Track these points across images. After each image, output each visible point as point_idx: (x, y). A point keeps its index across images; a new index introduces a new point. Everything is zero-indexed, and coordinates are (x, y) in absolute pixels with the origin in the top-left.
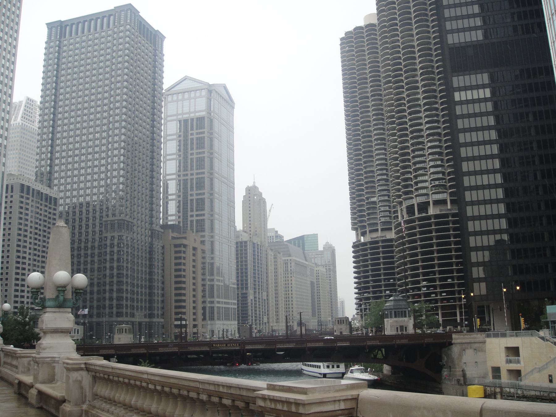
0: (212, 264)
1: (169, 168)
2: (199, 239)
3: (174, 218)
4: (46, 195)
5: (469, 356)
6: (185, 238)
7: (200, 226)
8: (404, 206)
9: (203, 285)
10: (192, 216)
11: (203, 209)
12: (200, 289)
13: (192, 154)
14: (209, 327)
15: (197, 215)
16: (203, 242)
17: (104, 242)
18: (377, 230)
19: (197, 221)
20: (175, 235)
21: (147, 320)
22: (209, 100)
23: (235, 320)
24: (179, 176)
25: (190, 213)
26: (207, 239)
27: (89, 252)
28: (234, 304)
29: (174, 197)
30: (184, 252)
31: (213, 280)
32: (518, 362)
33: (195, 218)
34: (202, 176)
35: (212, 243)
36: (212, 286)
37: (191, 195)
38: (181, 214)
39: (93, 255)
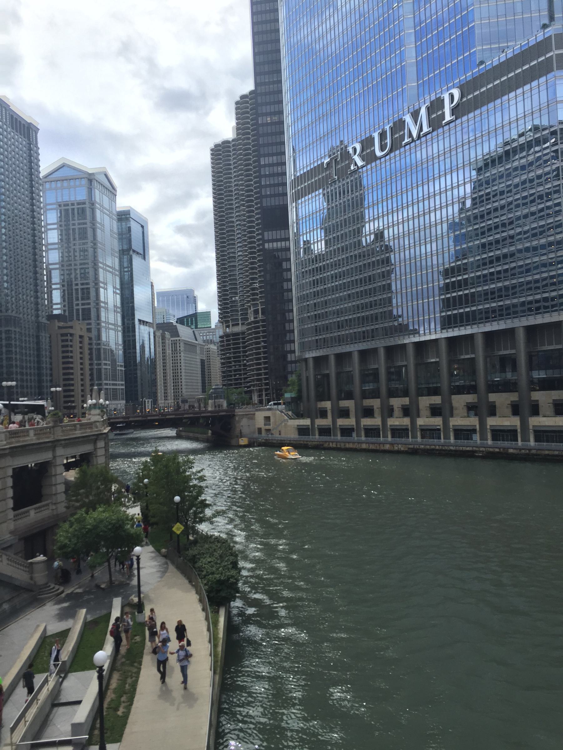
0: (99, 350)
1: (53, 257)
2: (85, 327)
3: (59, 306)
6: (71, 327)
7: (86, 315)
8: (252, 309)
9: (91, 370)
10: (78, 305)
11: (89, 298)
12: (88, 373)
15: (83, 304)
16: (89, 330)
18: (238, 324)
19: (83, 310)
20: (61, 324)
22: (90, 191)
23: (123, 399)
24: (63, 266)
25: (75, 303)
26: (93, 326)
28: (122, 385)
29: (58, 286)
30: (71, 341)
31: (100, 364)
32: (270, 425)
33: (80, 307)
35: (99, 331)
36: (99, 370)
37: (77, 285)
38: (66, 303)
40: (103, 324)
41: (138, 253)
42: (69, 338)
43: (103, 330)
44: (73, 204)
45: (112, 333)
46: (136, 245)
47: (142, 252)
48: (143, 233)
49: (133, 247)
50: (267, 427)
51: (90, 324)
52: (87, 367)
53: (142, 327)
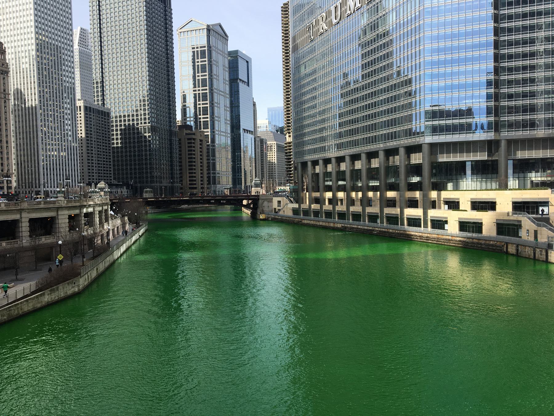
4: (102, 111)
5: (266, 203)
9: (208, 163)
13: (198, 76)
14: (213, 189)
17: (140, 140)
21: (170, 185)
27: (132, 145)
39: (134, 147)
40: (217, 132)
41: (243, 81)
44: (197, 48)
45: (223, 139)
46: (242, 75)
47: (246, 81)
49: (240, 77)
50: (279, 208)
52: (205, 162)
53: (246, 134)
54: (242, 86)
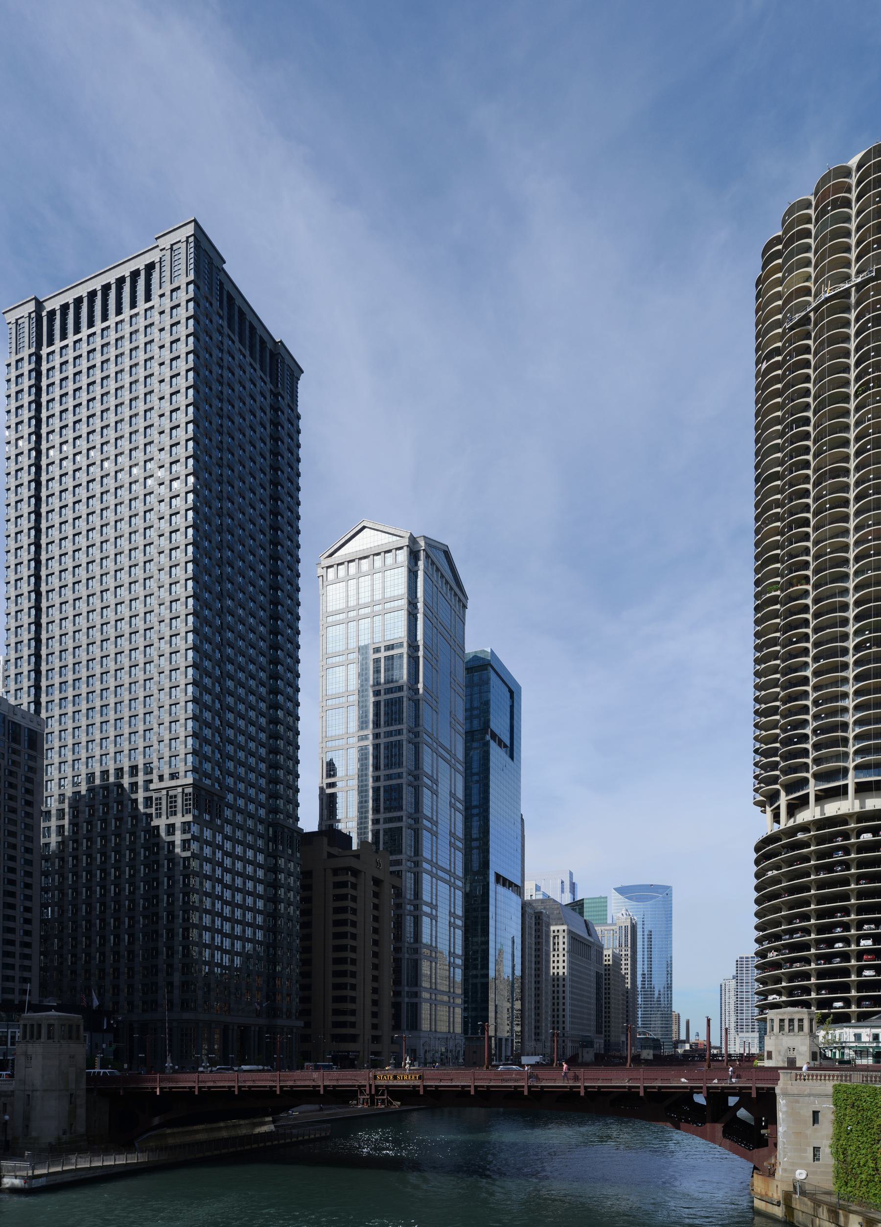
15: (387, 821)
34: (398, 738)
42: (351, 879)
43: (426, 878)
45: (443, 888)
46: (498, 723)
47: (508, 744)
48: (512, 707)
49: (493, 726)
51: (399, 863)
54: (496, 754)
